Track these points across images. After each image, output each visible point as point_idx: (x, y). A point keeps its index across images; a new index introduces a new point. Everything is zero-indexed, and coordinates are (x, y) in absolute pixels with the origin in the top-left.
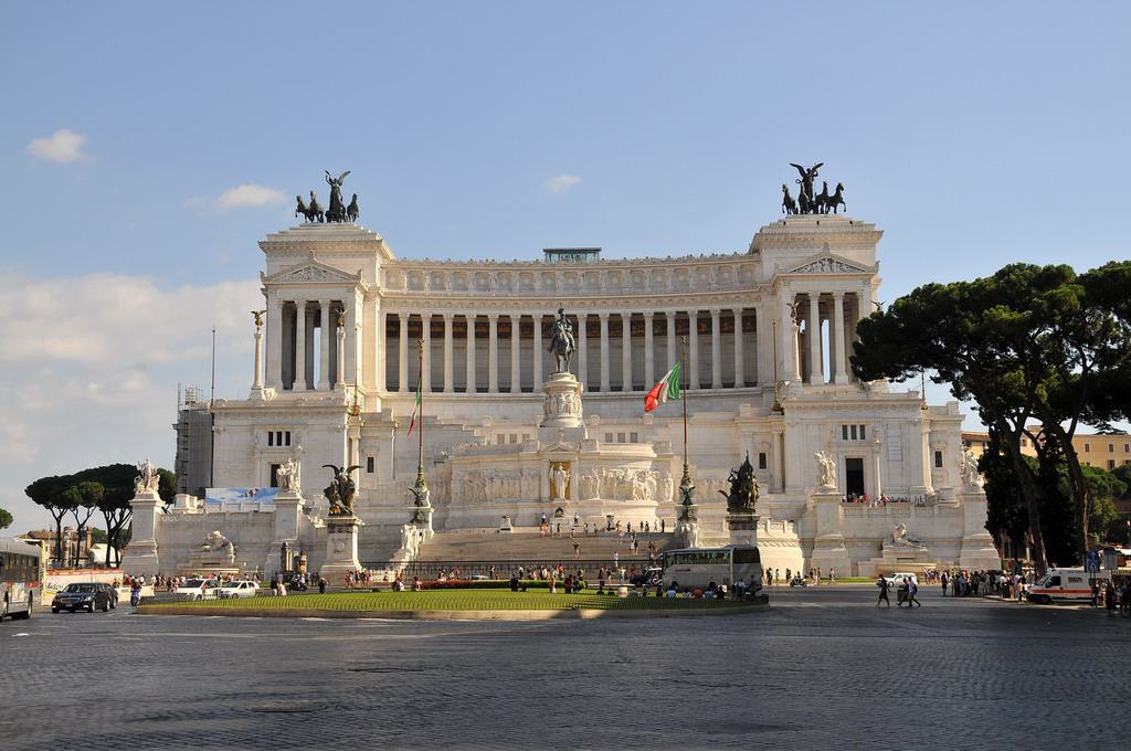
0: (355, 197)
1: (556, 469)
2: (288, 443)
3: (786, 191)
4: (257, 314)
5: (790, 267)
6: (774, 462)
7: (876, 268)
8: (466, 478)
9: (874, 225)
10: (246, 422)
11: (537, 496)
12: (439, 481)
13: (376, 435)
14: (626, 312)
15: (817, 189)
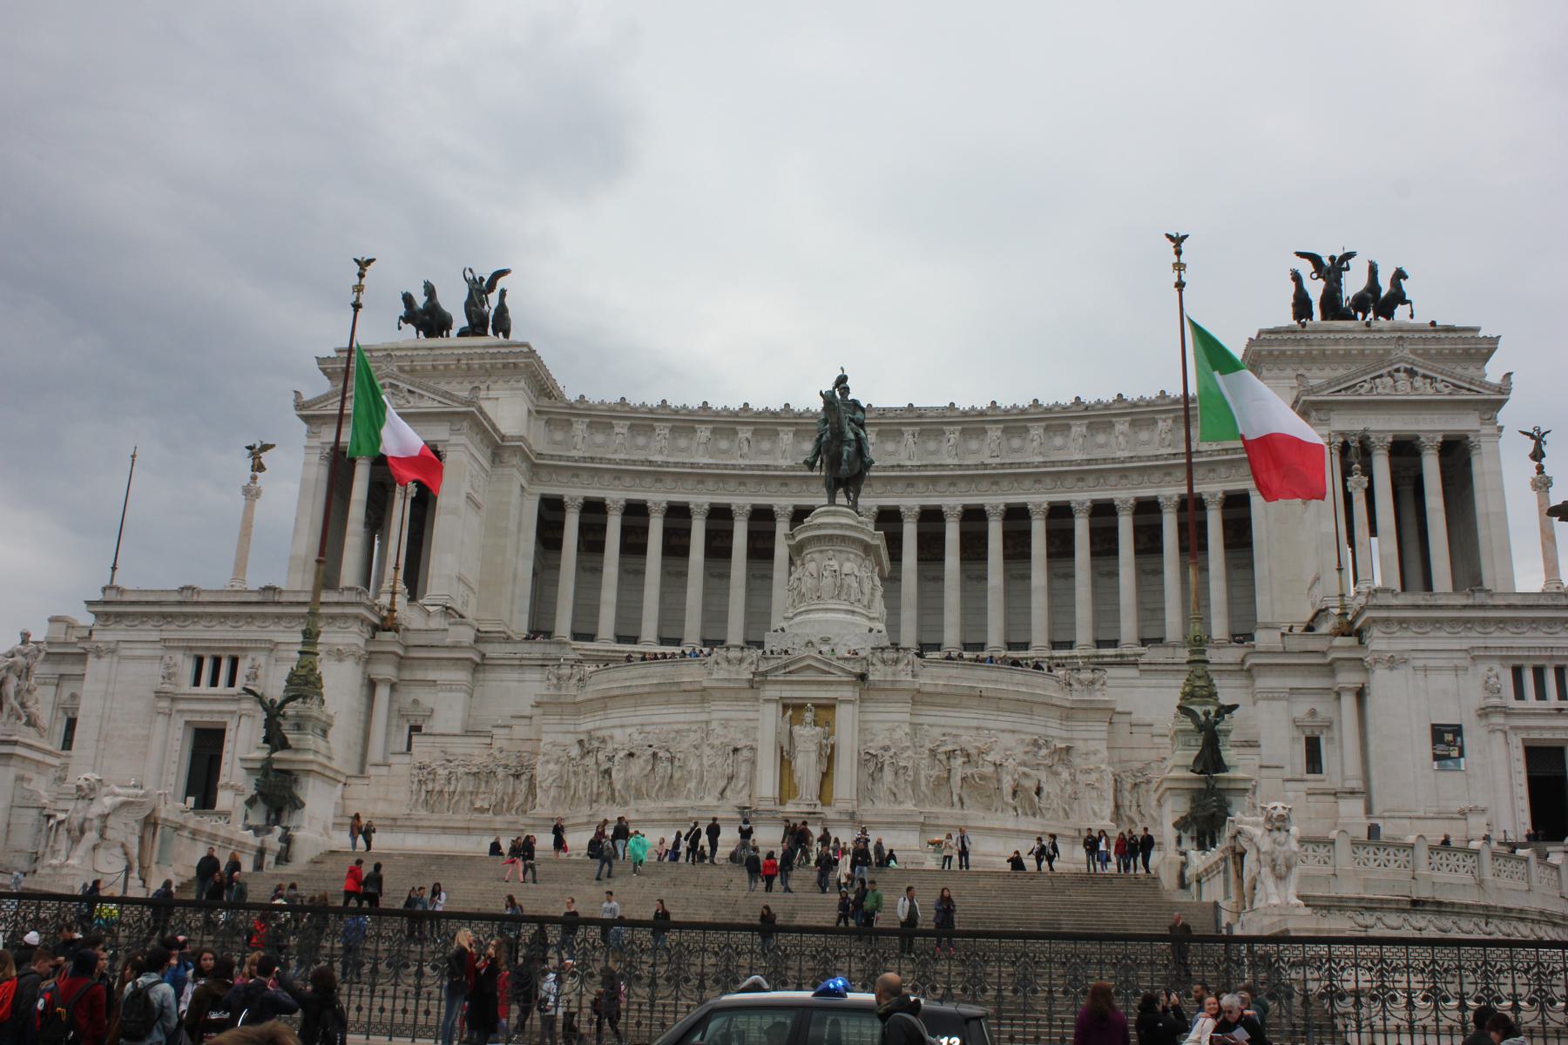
0: (503, 293)
1: (796, 720)
2: (231, 683)
3: (1296, 277)
4: (256, 453)
5: (1329, 384)
6: (1340, 761)
7: (1504, 388)
8: (575, 751)
9: (1477, 330)
10: (155, 636)
11: (743, 799)
12: (513, 762)
13: (431, 676)
14: (995, 501)
15: (1353, 284)
